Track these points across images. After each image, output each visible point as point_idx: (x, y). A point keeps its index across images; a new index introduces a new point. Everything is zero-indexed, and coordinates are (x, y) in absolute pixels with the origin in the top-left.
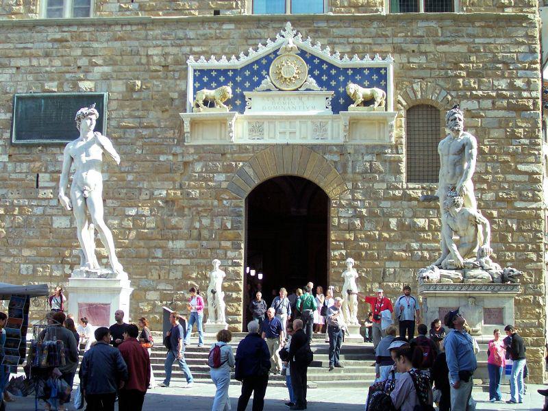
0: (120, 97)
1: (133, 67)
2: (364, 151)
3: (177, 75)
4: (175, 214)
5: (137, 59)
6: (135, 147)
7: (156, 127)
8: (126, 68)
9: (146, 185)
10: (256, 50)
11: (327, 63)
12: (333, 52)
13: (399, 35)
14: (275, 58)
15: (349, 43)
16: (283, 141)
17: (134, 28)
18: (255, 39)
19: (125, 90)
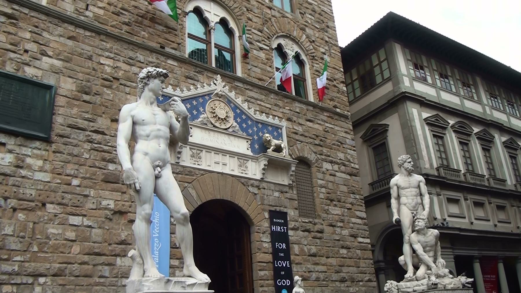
0: (68, 94)
1: (83, 70)
2: (273, 188)
3: (127, 90)
4: (123, 228)
5: (89, 64)
6: (83, 150)
7: (106, 135)
8: (78, 69)
9: (92, 193)
10: (196, 88)
11: (246, 115)
12: (249, 108)
13: (286, 108)
14: (209, 100)
15: (258, 104)
16: (218, 169)
17: (88, 33)
18: (195, 80)
19: (74, 89)
